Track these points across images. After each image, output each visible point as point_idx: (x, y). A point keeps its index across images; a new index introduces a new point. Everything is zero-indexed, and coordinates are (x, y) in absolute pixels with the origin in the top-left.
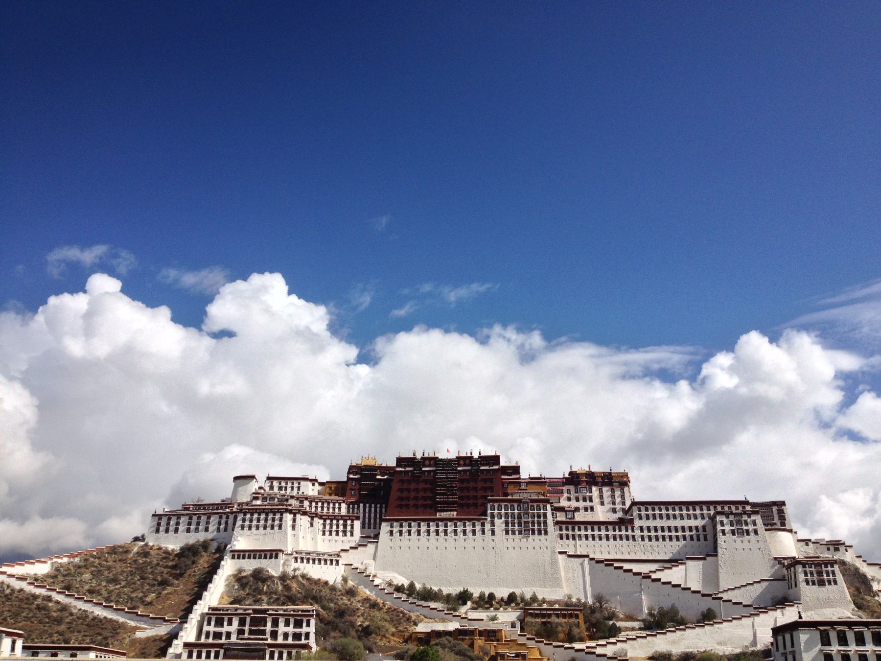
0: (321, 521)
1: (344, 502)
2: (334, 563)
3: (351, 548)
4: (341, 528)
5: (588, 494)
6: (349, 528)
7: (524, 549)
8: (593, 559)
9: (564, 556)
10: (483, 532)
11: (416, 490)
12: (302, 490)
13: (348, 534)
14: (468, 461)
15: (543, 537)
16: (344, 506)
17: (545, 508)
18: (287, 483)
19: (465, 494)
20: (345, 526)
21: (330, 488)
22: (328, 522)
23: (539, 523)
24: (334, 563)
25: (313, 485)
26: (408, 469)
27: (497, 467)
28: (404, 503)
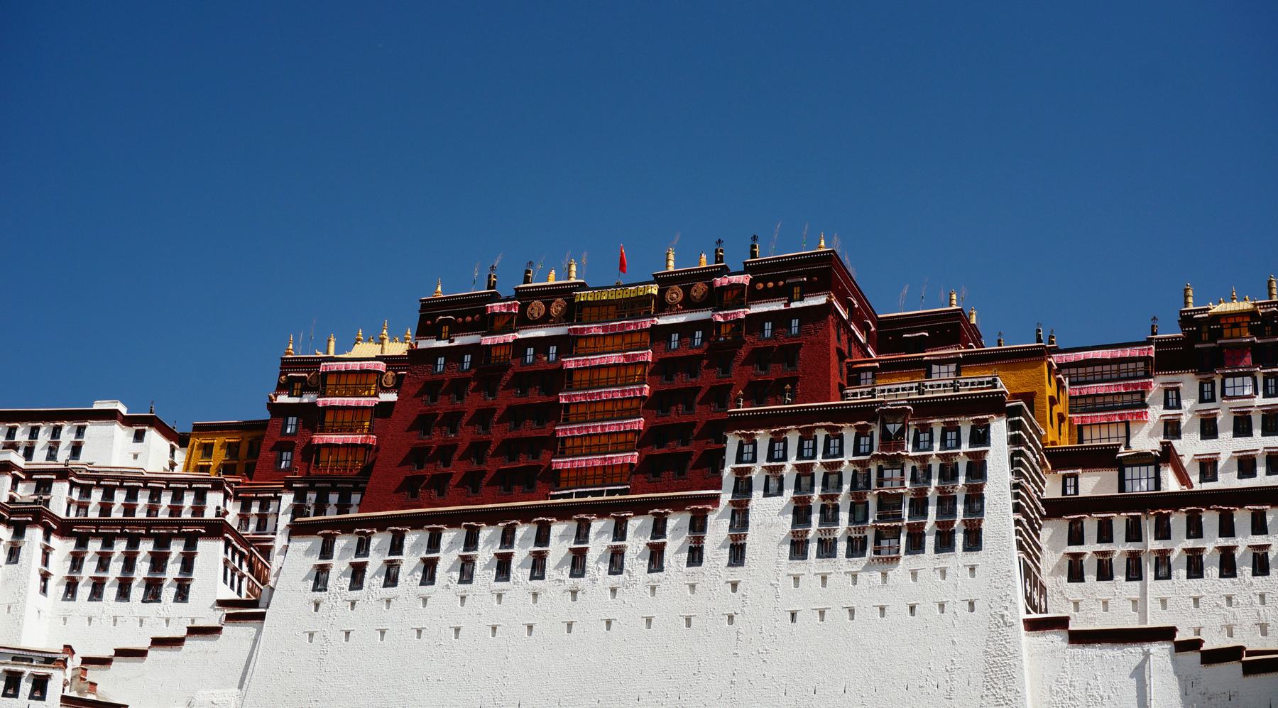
0: (71, 545)
1: (217, 486)
2: (26, 687)
3: (158, 642)
4: (142, 569)
5: (1259, 400)
6: (173, 570)
7: (868, 613)
8: (1194, 645)
9: (1056, 639)
10: (695, 556)
11: (483, 417)
12: (85, 457)
13: (169, 592)
14: (699, 289)
15: (959, 558)
16: (214, 500)
17: (981, 436)
18: (34, 433)
19: (676, 415)
20: (158, 561)
21: (207, 450)
22: (95, 546)
23: (946, 503)
24: (26, 687)
25: (139, 437)
26: (458, 341)
27: (821, 300)
28: (428, 471)
